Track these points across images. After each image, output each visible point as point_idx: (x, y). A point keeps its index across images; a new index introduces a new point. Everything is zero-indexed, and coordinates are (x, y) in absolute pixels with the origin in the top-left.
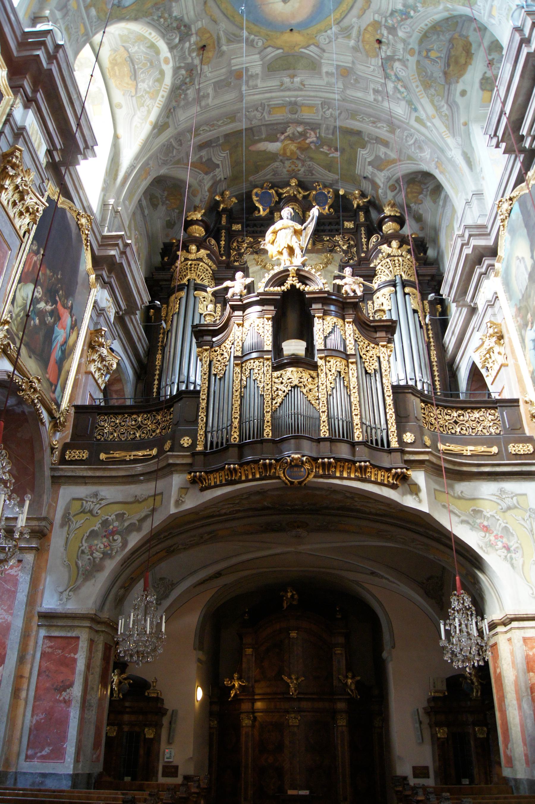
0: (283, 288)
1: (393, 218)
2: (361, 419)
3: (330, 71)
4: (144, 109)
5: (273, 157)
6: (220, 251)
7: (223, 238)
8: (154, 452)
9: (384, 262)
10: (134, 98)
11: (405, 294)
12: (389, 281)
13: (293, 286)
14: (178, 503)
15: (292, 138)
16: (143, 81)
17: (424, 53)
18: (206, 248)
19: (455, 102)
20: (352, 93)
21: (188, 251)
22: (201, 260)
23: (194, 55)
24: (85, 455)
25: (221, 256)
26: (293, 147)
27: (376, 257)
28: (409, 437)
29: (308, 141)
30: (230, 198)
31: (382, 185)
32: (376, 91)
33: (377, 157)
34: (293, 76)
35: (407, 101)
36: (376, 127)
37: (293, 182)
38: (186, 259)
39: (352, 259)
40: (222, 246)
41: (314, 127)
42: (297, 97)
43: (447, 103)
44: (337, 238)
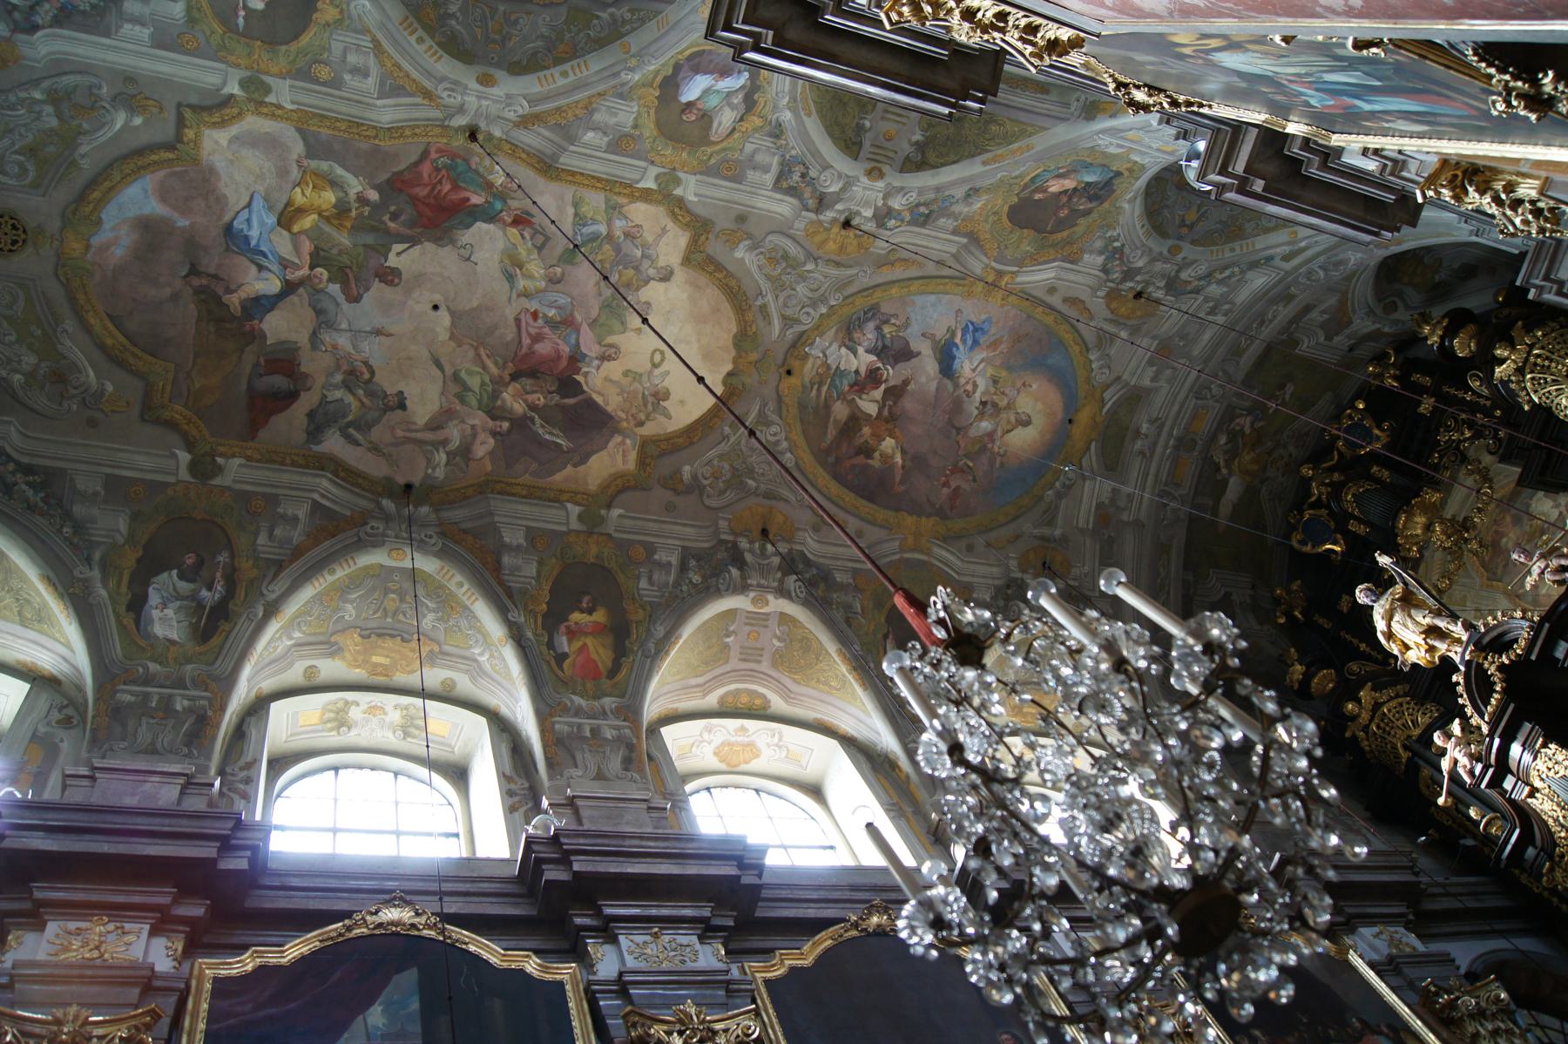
1: (1450, 332)
3: (1152, 374)
7: (1355, 641)
15: (1233, 454)
17: (1185, 231)
18: (1361, 687)
21: (1354, 718)
22: (1377, 706)
26: (1247, 457)
29: (1247, 430)
30: (1289, 592)
31: (1378, 326)
32: (1212, 312)
33: (1322, 326)
34: (1138, 433)
35: (1250, 269)
36: (1271, 321)
37: (1307, 471)
38: (1366, 728)
40: (1368, 649)
41: (1229, 414)
42: (1170, 435)
44: (1443, 438)
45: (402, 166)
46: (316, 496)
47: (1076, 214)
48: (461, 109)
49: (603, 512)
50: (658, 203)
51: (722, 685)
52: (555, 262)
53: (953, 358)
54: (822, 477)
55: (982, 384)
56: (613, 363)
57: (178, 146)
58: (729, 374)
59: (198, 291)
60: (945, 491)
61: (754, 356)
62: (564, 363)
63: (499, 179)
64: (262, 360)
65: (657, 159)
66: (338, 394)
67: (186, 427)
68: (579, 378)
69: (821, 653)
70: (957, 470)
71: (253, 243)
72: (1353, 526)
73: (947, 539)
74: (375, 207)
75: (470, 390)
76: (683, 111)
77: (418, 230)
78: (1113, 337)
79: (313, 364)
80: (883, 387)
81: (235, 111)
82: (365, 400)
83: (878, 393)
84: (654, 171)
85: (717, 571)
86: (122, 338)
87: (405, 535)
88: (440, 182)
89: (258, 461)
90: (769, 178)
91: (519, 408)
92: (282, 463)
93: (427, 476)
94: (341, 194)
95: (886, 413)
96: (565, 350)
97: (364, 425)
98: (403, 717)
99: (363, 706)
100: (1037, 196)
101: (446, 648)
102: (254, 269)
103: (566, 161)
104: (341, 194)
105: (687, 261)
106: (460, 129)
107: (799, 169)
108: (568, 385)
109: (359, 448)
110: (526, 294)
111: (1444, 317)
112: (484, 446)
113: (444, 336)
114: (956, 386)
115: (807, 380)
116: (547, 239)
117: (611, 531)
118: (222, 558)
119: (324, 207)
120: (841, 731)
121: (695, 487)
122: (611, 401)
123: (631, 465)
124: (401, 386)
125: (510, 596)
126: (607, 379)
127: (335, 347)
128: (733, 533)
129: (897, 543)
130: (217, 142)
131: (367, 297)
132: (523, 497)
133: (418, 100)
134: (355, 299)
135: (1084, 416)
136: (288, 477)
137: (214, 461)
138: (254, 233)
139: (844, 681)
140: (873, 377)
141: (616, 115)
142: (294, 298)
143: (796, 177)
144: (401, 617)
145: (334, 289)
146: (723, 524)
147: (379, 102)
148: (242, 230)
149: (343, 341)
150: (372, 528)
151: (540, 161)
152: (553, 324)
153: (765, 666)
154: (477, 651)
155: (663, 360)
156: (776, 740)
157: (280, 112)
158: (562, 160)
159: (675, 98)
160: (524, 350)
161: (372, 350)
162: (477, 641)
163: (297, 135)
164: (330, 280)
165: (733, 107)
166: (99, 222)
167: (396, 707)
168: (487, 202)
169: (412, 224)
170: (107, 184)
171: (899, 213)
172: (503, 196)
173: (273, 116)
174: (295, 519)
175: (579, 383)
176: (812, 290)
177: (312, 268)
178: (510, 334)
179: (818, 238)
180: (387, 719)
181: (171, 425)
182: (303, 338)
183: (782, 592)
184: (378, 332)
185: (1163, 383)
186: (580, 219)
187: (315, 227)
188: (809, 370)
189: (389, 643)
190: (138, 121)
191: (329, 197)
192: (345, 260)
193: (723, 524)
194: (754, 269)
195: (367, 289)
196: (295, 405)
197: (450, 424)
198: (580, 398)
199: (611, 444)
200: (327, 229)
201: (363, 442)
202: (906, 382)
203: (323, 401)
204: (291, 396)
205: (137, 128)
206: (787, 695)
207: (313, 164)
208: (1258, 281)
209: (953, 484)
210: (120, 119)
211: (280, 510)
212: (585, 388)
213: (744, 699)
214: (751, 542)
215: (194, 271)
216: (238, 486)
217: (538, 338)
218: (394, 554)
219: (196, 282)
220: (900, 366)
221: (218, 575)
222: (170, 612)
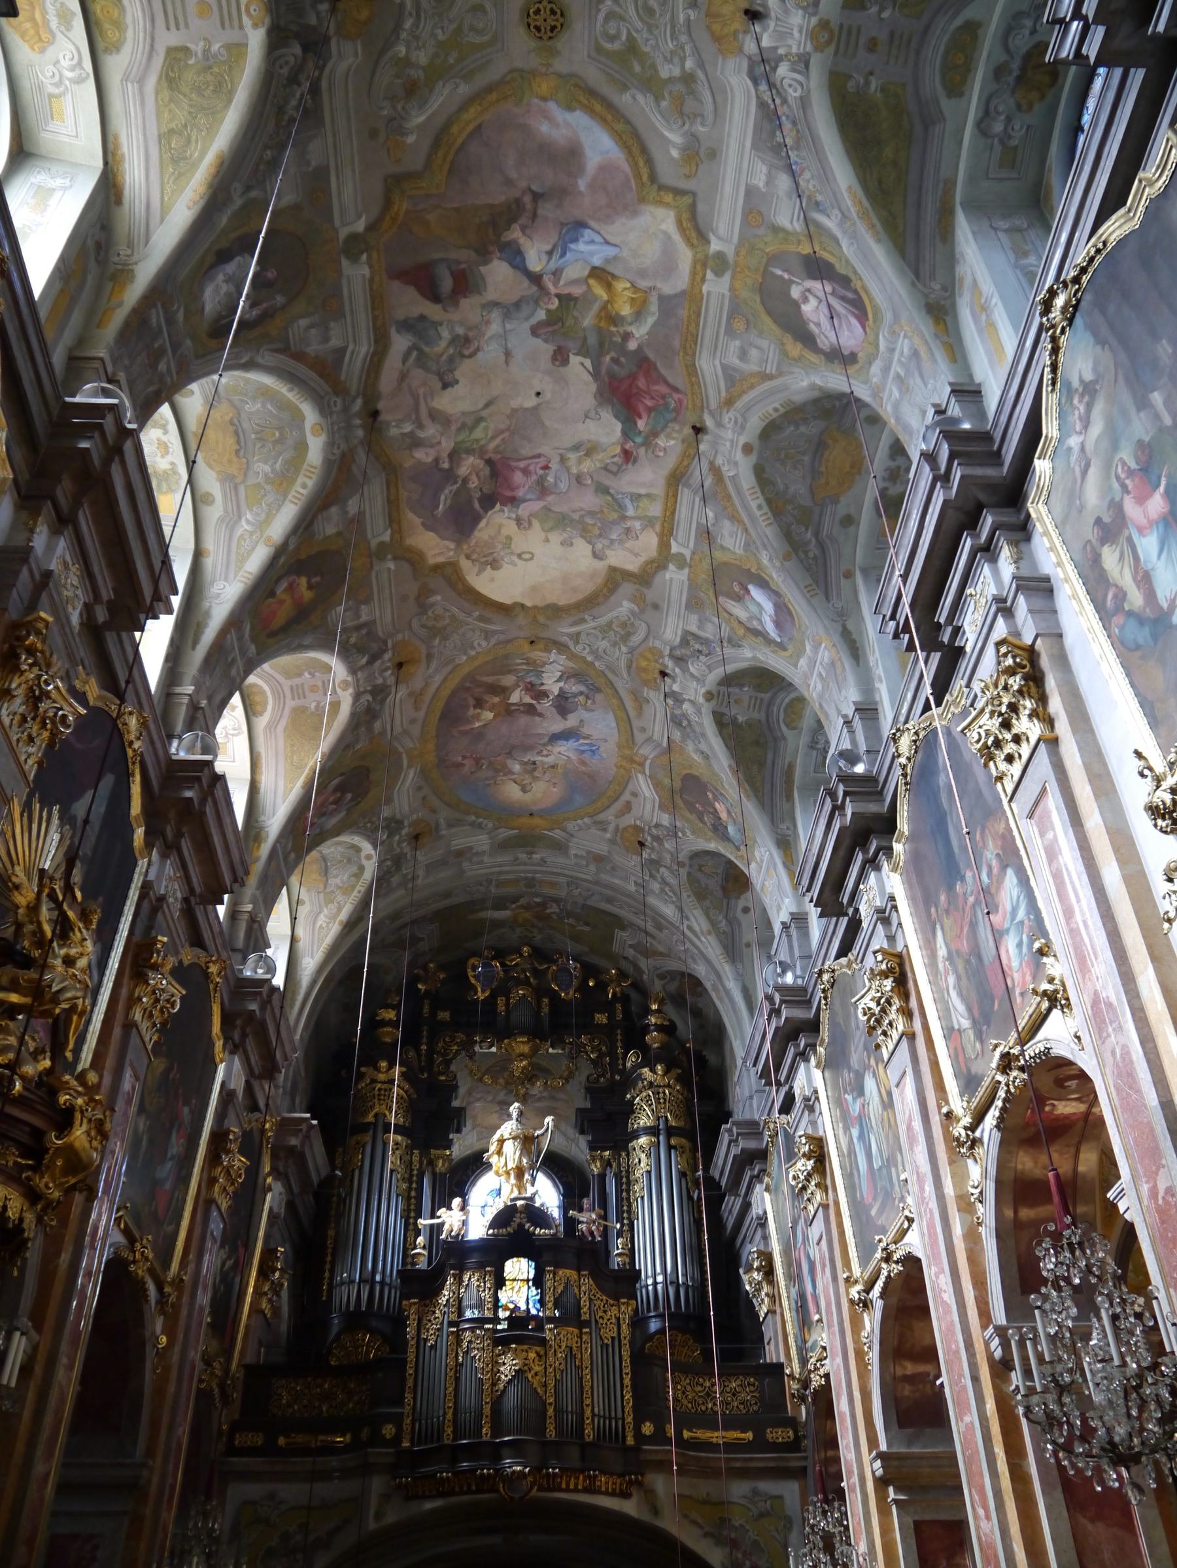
0: (510, 1229)
1: (658, 1028)
2: (593, 1410)
4: (333, 907)
5: (497, 924)
6: (420, 1062)
7: (425, 1040)
9: (644, 1094)
10: (322, 895)
11: (670, 1147)
12: (650, 1128)
15: (527, 907)
16: (336, 877)
17: (696, 867)
19: (736, 918)
20: (604, 877)
21: (377, 1069)
23: (405, 844)
24: (259, 1440)
25: (422, 1071)
27: (634, 1085)
28: (648, 1429)
29: (548, 911)
38: (374, 1081)
39: (603, 1075)
41: (556, 900)
42: (536, 872)
43: (726, 917)
44: (584, 1039)
45: (663, 371)
46: (351, 347)
48: (719, 425)
49: (390, 556)
50: (660, 552)
51: (265, 681)
52: (595, 478)
53: (567, 739)
54: (452, 684)
55: (550, 760)
56: (516, 527)
57: (655, 187)
58: (523, 606)
59: (518, 202)
60: (460, 759)
61: (542, 619)
62: (509, 494)
63: (661, 442)
64: (463, 266)
65: (697, 557)
66: (446, 334)
67: (388, 218)
68: (498, 506)
69: (315, 739)
70: (477, 761)
71: (572, 246)
72: (501, 1001)
73: (424, 773)
74: (622, 348)
75: (471, 433)
76: (740, 584)
77: (607, 380)
78: (605, 830)
79: (469, 307)
80: (534, 702)
81: (695, 242)
82: (445, 357)
83: (528, 700)
84: (687, 554)
85: (361, 649)
86: (460, 141)
87: (336, 427)
88: (652, 398)
89: (371, 289)
90: (693, 628)
91: (463, 470)
92: (373, 309)
93: (388, 424)
94: (629, 320)
95: (513, 708)
96: (520, 493)
97: (422, 361)
98: (165, 472)
99: (165, 438)
100: (710, 795)
101: (242, 489)
102: (548, 247)
103: (686, 497)
104: (629, 320)
105: (613, 570)
106: (702, 421)
107: (704, 649)
108: (489, 501)
109: (400, 364)
110: (563, 460)
111: (670, 1020)
112: (423, 456)
113: (515, 403)
114: (544, 745)
115: (529, 655)
116: (615, 474)
117: (376, 568)
118: (280, 299)
119: (616, 306)
120: (257, 777)
121: (423, 607)
122: (483, 532)
123: (432, 561)
124: (462, 380)
125: (306, 529)
126: (500, 526)
127: (488, 322)
128: (393, 648)
129: (411, 745)
130: (663, 221)
131: (538, 342)
132: (388, 497)
133: (723, 394)
134: (534, 331)
135: (536, 821)
136: (363, 319)
137: (362, 253)
138: (581, 246)
139: (301, 767)
140: (541, 695)
141: (731, 536)
142: (526, 283)
143: (697, 646)
144: (259, 445)
145: (541, 315)
146: (400, 637)
147: (717, 362)
148: (583, 236)
149: (495, 328)
150: (335, 402)
151: (683, 475)
152: (541, 482)
153: (291, 703)
154: (249, 516)
155: (526, 560)
156: (232, 732)
157: (698, 278)
158: (686, 491)
159: (751, 582)
160: (514, 464)
161: (491, 352)
162: (258, 515)
163: (679, 290)
164: (548, 311)
165: (750, 618)
166: (570, 108)
167: (172, 463)
168: (640, 432)
169: (612, 376)
170: (609, 117)
171: (681, 707)
172: (647, 443)
173: (694, 274)
174: (326, 339)
175: (493, 507)
176: (604, 651)
177: (558, 296)
178: (526, 451)
179: (649, 656)
180: (158, 459)
181: (388, 203)
182: (491, 295)
183: (357, 697)
184: (508, 354)
185: (573, 861)
186: (636, 498)
187: (596, 298)
188: (537, 655)
189: (231, 441)
190: (675, 153)
191: (626, 311)
192: (569, 322)
193: (400, 637)
194: (614, 614)
195: (546, 341)
196: (429, 304)
197: (438, 426)
198: (481, 511)
199: (447, 543)
200: (596, 307)
201: (407, 364)
202: (540, 715)
203: (436, 324)
204: (436, 298)
205: (668, 152)
206: (272, 726)
207: (654, 299)
208: (669, 911)
209: (465, 762)
210: (675, 138)
211: (332, 324)
212: (490, 513)
213: (257, 699)
214: (389, 660)
215: (537, 197)
216: (344, 282)
217: (526, 472)
218: (318, 427)
219: (527, 199)
220: (554, 710)
221: (265, 305)
222: (224, 288)
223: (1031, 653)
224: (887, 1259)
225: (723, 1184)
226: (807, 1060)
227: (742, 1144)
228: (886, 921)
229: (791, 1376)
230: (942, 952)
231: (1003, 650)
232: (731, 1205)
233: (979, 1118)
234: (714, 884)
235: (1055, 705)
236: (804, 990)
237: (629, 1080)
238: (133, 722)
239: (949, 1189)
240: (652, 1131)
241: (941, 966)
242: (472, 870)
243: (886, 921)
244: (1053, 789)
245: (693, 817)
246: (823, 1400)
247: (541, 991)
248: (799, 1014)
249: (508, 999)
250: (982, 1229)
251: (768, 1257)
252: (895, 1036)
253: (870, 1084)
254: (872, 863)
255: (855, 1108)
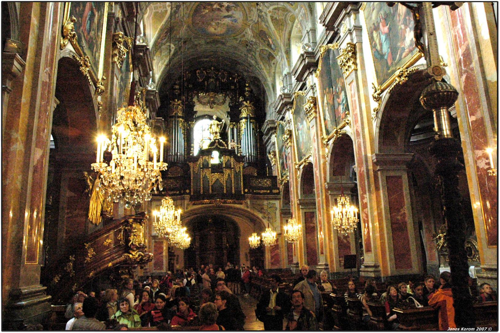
1: (248, 91)
4: (163, 61)
8: (178, 192)
11: (250, 122)
13: (217, 146)
14: (187, 208)
18: (181, 100)
21: (175, 101)
22: (179, 105)
27: (242, 106)
28: (246, 190)
38: (174, 105)
47: (264, 41)
208: (253, 62)
223: (355, 45)
224: (305, 162)
225: (265, 133)
226: (289, 111)
227: (270, 126)
228: (313, 89)
229: (279, 179)
230: (325, 101)
231: (349, 45)
232: (265, 138)
233: (329, 140)
234: (266, 57)
235: (358, 61)
236: (289, 94)
237: (241, 104)
238: (130, 41)
239: (321, 153)
240: (246, 118)
241: (325, 104)
242: (200, 49)
243: (313, 89)
244: (355, 81)
245: (262, 41)
246: (287, 186)
247: (217, 79)
248: (287, 100)
249: (208, 82)
250: (327, 163)
251: (275, 152)
252: (313, 117)
253: (305, 122)
254: (311, 73)
255: (301, 127)
